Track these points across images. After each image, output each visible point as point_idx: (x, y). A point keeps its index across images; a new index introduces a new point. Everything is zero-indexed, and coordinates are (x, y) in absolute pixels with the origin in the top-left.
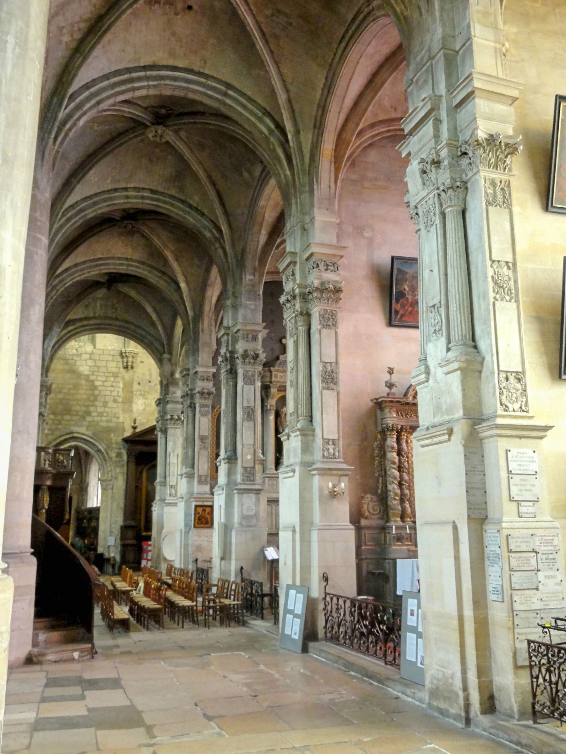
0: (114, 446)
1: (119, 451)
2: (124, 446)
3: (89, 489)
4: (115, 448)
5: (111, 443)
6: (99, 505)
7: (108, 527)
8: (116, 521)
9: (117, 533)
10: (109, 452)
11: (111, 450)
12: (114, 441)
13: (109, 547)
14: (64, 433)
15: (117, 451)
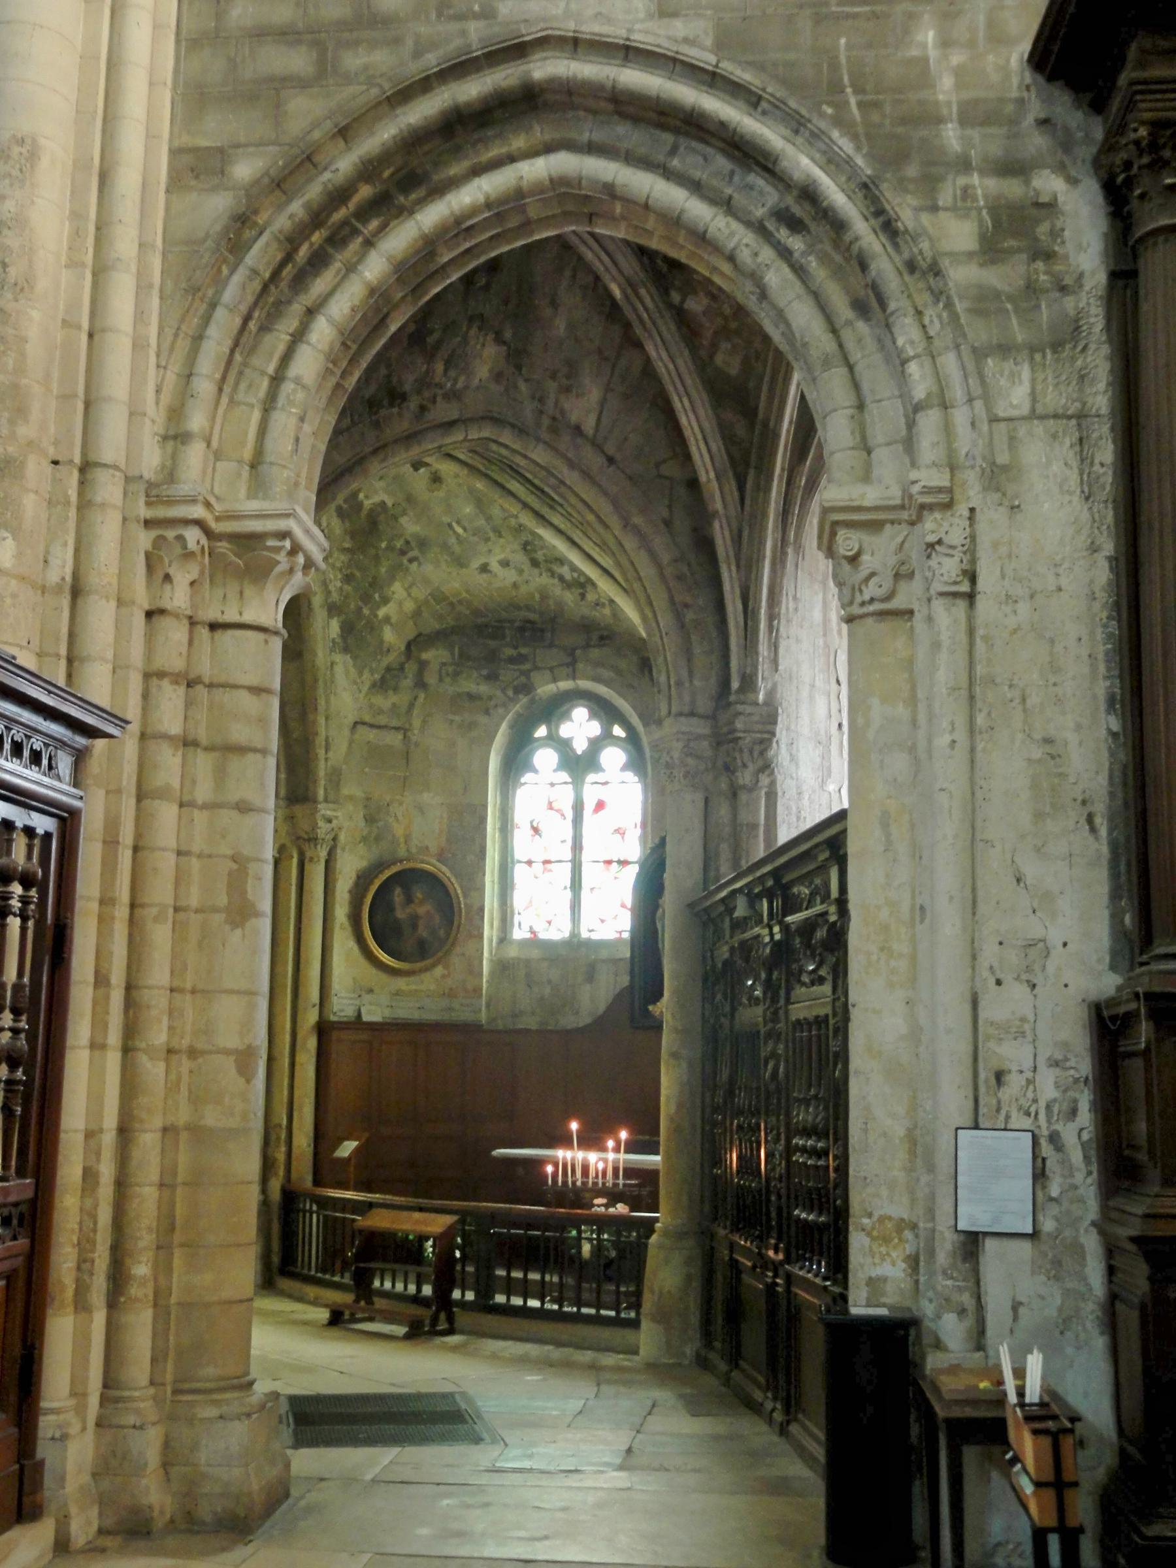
0: (951, 136)
1: (1013, 189)
2: (1066, 145)
3: (781, 753)
4: (964, 165)
5: (933, 118)
6: (846, 805)
7: (954, 1016)
8: (1037, 948)
9: (1048, 1087)
10: (905, 210)
11: (929, 183)
12: (945, 88)
13: (971, 1244)
14: (432, 61)
15: (983, 186)
